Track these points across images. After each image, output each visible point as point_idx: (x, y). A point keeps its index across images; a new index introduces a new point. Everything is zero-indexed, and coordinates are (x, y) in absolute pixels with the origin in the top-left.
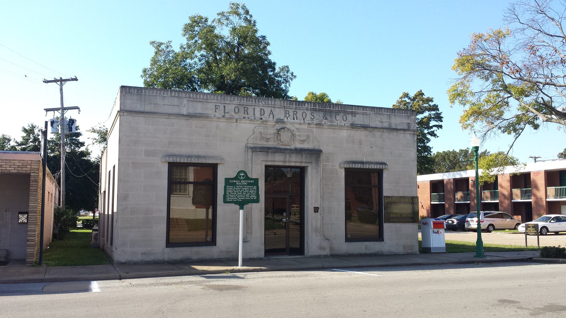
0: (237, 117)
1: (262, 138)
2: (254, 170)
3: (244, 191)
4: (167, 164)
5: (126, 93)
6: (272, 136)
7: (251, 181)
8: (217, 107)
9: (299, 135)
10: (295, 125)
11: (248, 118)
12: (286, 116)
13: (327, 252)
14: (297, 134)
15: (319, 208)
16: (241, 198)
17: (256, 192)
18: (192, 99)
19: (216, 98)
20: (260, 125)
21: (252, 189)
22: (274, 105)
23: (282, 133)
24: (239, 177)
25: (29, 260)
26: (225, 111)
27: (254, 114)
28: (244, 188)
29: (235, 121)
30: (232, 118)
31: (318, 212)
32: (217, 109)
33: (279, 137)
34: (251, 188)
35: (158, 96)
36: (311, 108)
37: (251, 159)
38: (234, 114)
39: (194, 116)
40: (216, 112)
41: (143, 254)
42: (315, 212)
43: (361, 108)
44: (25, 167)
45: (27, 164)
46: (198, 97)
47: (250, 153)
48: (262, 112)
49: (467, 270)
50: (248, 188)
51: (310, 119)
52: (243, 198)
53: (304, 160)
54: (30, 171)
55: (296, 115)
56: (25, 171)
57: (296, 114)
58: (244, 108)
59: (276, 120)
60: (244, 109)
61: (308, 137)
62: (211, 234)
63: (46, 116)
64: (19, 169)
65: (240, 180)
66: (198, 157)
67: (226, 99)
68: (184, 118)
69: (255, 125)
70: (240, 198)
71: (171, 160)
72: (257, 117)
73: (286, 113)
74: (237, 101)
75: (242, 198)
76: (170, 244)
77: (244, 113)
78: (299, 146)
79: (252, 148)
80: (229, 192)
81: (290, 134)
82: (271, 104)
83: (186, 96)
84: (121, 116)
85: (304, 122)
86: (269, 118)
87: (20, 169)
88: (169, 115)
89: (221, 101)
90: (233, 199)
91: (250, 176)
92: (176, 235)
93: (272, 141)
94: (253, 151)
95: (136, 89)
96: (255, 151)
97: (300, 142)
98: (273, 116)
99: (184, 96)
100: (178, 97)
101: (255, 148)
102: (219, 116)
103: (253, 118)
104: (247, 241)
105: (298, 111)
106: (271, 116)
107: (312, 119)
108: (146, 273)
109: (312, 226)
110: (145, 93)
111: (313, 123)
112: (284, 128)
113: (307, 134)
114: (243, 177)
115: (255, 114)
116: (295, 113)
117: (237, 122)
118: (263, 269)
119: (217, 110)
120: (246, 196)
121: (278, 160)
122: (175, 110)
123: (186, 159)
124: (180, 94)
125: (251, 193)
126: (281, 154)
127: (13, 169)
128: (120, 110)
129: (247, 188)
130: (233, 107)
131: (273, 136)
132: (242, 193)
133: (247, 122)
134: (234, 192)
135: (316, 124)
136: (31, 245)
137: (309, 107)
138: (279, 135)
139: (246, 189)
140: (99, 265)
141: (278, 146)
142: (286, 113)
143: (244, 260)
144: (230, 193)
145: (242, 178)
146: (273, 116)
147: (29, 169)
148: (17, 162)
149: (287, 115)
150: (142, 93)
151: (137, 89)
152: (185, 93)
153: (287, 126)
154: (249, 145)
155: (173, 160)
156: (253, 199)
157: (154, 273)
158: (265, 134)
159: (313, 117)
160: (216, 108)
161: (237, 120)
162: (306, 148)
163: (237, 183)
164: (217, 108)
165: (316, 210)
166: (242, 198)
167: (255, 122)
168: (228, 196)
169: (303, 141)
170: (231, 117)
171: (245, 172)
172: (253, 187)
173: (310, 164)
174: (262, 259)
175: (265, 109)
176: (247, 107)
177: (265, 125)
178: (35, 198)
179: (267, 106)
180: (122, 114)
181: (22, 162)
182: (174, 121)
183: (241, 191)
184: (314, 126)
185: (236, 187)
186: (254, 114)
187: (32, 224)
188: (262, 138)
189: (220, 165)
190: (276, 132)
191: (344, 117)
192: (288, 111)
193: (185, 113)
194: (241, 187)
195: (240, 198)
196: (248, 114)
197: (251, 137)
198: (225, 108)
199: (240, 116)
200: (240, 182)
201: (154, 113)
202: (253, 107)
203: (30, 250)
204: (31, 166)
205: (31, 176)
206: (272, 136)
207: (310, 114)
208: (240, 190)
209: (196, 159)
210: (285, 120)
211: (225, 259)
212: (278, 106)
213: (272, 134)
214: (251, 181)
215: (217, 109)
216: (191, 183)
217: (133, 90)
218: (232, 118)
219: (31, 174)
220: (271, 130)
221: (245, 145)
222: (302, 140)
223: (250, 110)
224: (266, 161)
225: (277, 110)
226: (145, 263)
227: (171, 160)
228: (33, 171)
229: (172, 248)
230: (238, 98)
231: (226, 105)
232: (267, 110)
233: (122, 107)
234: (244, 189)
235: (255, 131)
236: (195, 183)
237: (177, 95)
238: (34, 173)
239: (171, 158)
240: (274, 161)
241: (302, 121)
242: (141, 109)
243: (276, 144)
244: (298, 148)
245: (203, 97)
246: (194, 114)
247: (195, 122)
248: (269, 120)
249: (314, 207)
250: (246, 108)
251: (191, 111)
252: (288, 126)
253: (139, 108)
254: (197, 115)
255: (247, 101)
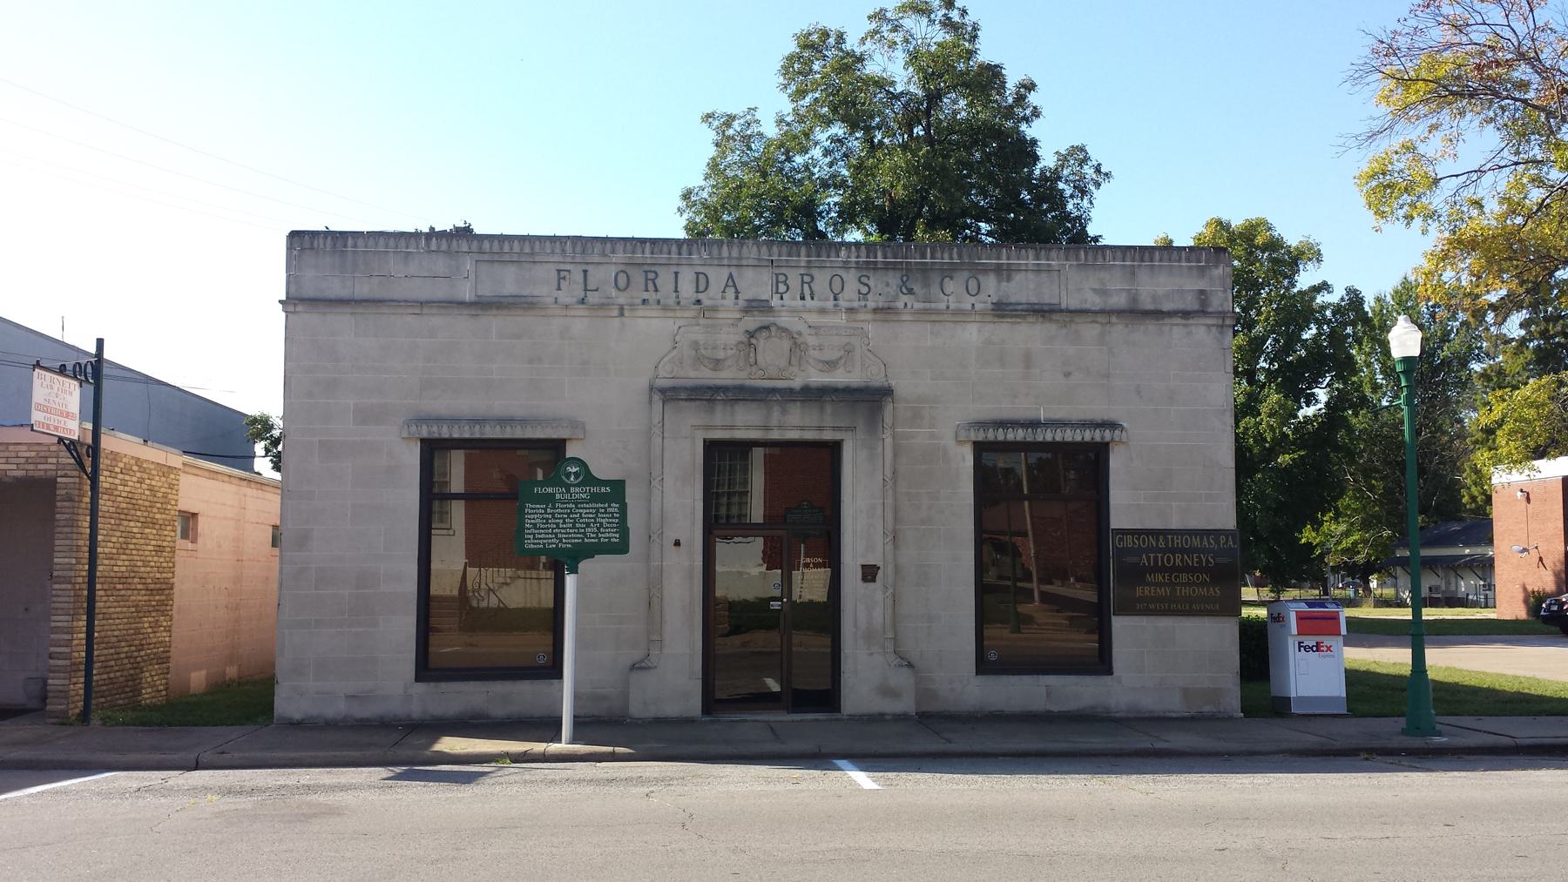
0: (622, 300)
1: (699, 360)
2: (667, 455)
3: (581, 517)
4: (416, 443)
5: (303, 249)
6: (730, 352)
7: (603, 490)
8: (562, 274)
9: (820, 346)
10: (805, 316)
11: (659, 302)
12: (777, 288)
13: (906, 705)
14: (810, 344)
15: (879, 568)
16: (569, 538)
17: (617, 521)
18: (486, 257)
19: (558, 250)
20: (694, 321)
21: (605, 513)
22: (740, 258)
23: (761, 342)
24: (563, 477)
25: (53, 707)
26: (586, 285)
27: (676, 287)
28: (581, 511)
29: (616, 313)
30: (609, 305)
31: (874, 580)
32: (561, 280)
33: (752, 355)
34: (603, 510)
35: (392, 255)
36: (857, 263)
37: (661, 424)
38: (614, 293)
39: (494, 303)
40: (559, 289)
41: (351, 697)
42: (865, 579)
43: (619, 247)
44: (43, 460)
45: (47, 454)
46: (506, 249)
47: (658, 405)
48: (702, 283)
49: (1260, 779)
50: (592, 508)
51: (855, 296)
52: (577, 538)
53: (828, 421)
54: (54, 473)
55: (810, 288)
56: (42, 473)
57: (809, 283)
58: (646, 272)
59: (745, 304)
60: (646, 276)
61: (848, 350)
62: (552, 643)
63: (63, 317)
64: (27, 467)
65: (568, 487)
66: (503, 421)
67: (590, 252)
68: (466, 312)
69: (680, 323)
70: (565, 538)
71: (425, 434)
72: (686, 299)
73: (777, 282)
74: (621, 255)
75: (574, 538)
76: (426, 669)
77: (644, 288)
78: (817, 378)
79: (663, 391)
80: (532, 521)
81: (786, 344)
82: (728, 258)
83: (470, 248)
84: (290, 315)
85: (836, 306)
86: (723, 298)
87: (31, 467)
88: (422, 304)
89: (573, 257)
90: (544, 544)
91: (597, 472)
92: (448, 646)
93: (730, 366)
94: (668, 400)
95: (329, 238)
96: (672, 399)
97: (820, 366)
98: (737, 292)
99: (465, 247)
100: (448, 253)
101: (674, 389)
102: (568, 300)
103: (671, 301)
104: (649, 668)
105: (815, 272)
106: (731, 292)
107: (863, 296)
108: (267, 755)
109: (856, 625)
110: (355, 246)
111: (865, 306)
112: (767, 328)
113: (845, 340)
114: (576, 478)
115: (679, 290)
116: (807, 280)
117: (622, 314)
118: (618, 754)
119: (564, 284)
120: (584, 534)
121: (744, 423)
122: (441, 291)
123: (467, 428)
124: (454, 242)
125: (601, 524)
126: (754, 405)
127: (14, 467)
128: (287, 298)
129: (589, 508)
130: (613, 270)
131: (733, 351)
132: (574, 524)
133: (654, 314)
134: (547, 523)
135: (876, 310)
136: (57, 668)
137: (853, 259)
138: (753, 350)
139: (587, 512)
140: (232, 725)
141: (748, 383)
142: (779, 281)
143: (578, 722)
144: (535, 525)
145: (572, 479)
146: (737, 292)
147: (54, 467)
148: (24, 448)
149: (782, 288)
150: (345, 246)
151: (332, 238)
152: (447, 240)
153: (777, 320)
154: (661, 383)
155: (429, 432)
156: (610, 540)
157: (293, 755)
158: (710, 347)
159: (864, 290)
160: (559, 279)
161: (622, 309)
162: (840, 386)
163: (558, 497)
164: (564, 278)
165: (869, 573)
166: (574, 538)
167: (679, 314)
168: (530, 534)
169: (831, 365)
170: (603, 301)
171: (579, 459)
172: (609, 506)
173: (850, 433)
174: (693, 721)
175: (711, 272)
176: (653, 269)
177: (709, 322)
178: (67, 542)
179: (716, 262)
180: (291, 308)
181: (36, 448)
182: (437, 320)
183: (571, 519)
184: (869, 316)
185: (554, 508)
186: (676, 287)
187: (60, 612)
188: (699, 360)
189: (575, 442)
190: (744, 339)
191: (619, 278)
192: (785, 275)
193: (468, 296)
194: (571, 506)
195: (565, 538)
196: (656, 290)
197: (666, 359)
198: (588, 277)
199: (633, 298)
200: (568, 491)
201: (380, 301)
202: (675, 269)
203: (57, 682)
204: (57, 457)
205: (58, 485)
206: (730, 352)
207: (857, 280)
208: (565, 516)
209: (498, 427)
210: (775, 302)
211: (589, 717)
212: (751, 262)
213: (732, 347)
214: (603, 490)
215: (561, 280)
216: (457, 496)
217: (321, 241)
218: (609, 305)
219: (59, 480)
220: (729, 333)
221: (647, 385)
222: (827, 360)
223: (665, 279)
224: (708, 428)
225: (749, 274)
226: (355, 723)
227: (425, 432)
228: (63, 472)
229: (432, 684)
230: (625, 245)
231: (590, 268)
232: (717, 276)
233: (293, 289)
234: (581, 514)
235: (677, 338)
236: (467, 497)
237: (444, 247)
238: (65, 476)
239: (424, 427)
240: (732, 427)
241: (830, 304)
242: (344, 293)
243: (743, 375)
244: (813, 385)
245: (521, 250)
246: (495, 300)
247: (495, 322)
248: (722, 305)
249: (863, 566)
250: (651, 271)
251: (487, 291)
252: (784, 319)
253: (335, 289)
254: (502, 299)
255: (652, 253)
